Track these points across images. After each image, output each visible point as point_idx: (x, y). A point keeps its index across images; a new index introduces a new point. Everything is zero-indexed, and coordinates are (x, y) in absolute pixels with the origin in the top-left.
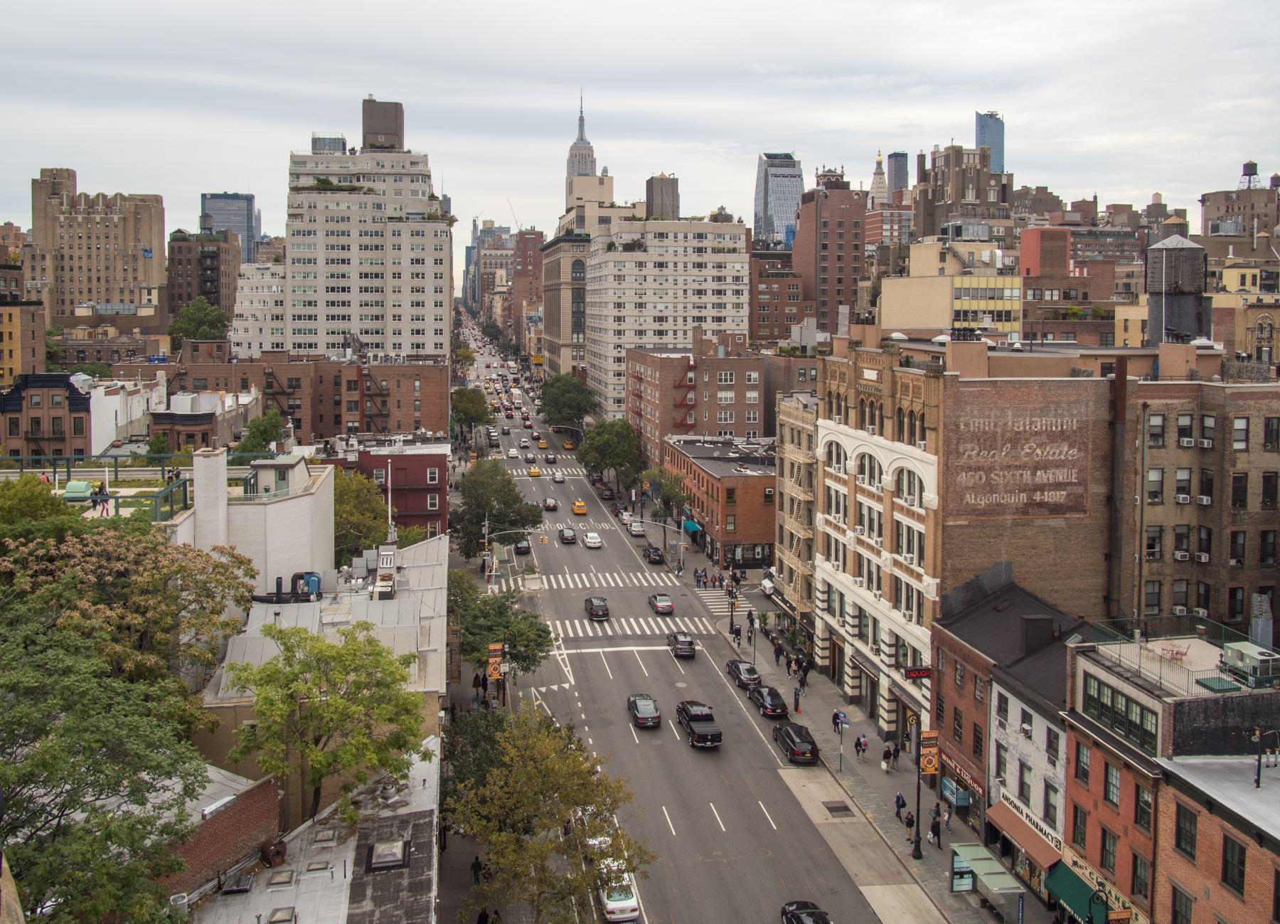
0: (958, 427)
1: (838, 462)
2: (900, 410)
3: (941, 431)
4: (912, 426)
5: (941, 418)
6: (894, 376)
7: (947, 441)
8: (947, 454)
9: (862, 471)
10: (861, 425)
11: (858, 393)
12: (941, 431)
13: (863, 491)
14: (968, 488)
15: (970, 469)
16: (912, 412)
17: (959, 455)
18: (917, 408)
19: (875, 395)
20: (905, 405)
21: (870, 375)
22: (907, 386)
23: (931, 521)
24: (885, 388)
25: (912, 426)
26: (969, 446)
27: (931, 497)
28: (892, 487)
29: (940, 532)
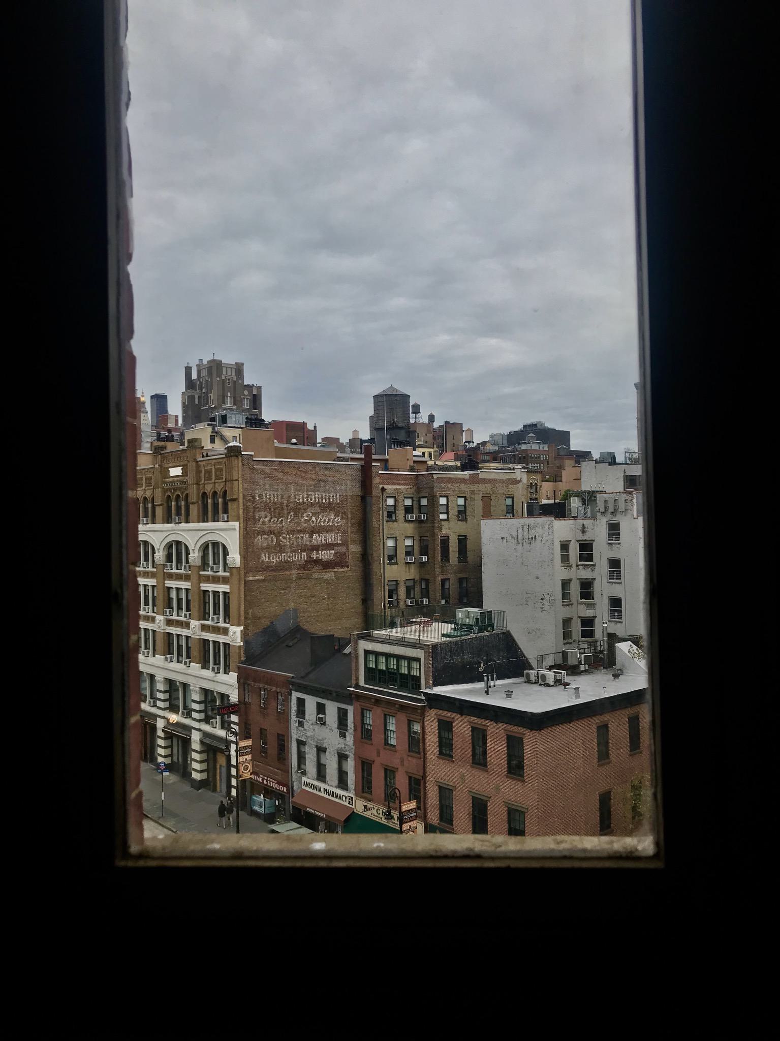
0: (254, 498)
1: (146, 559)
2: (204, 494)
3: (241, 500)
4: (215, 506)
5: (241, 490)
6: (198, 467)
7: (246, 509)
8: (246, 520)
9: (169, 558)
10: (168, 519)
11: (165, 491)
12: (241, 500)
13: (171, 576)
14: (263, 548)
15: (264, 533)
16: (215, 493)
17: (256, 521)
18: (219, 488)
19: (180, 489)
20: (209, 488)
21: (176, 471)
22: (209, 472)
23: (235, 580)
24: (190, 479)
25: (215, 506)
26: (263, 514)
27: (235, 557)
28: (198, 562)
29: (242, 586)
